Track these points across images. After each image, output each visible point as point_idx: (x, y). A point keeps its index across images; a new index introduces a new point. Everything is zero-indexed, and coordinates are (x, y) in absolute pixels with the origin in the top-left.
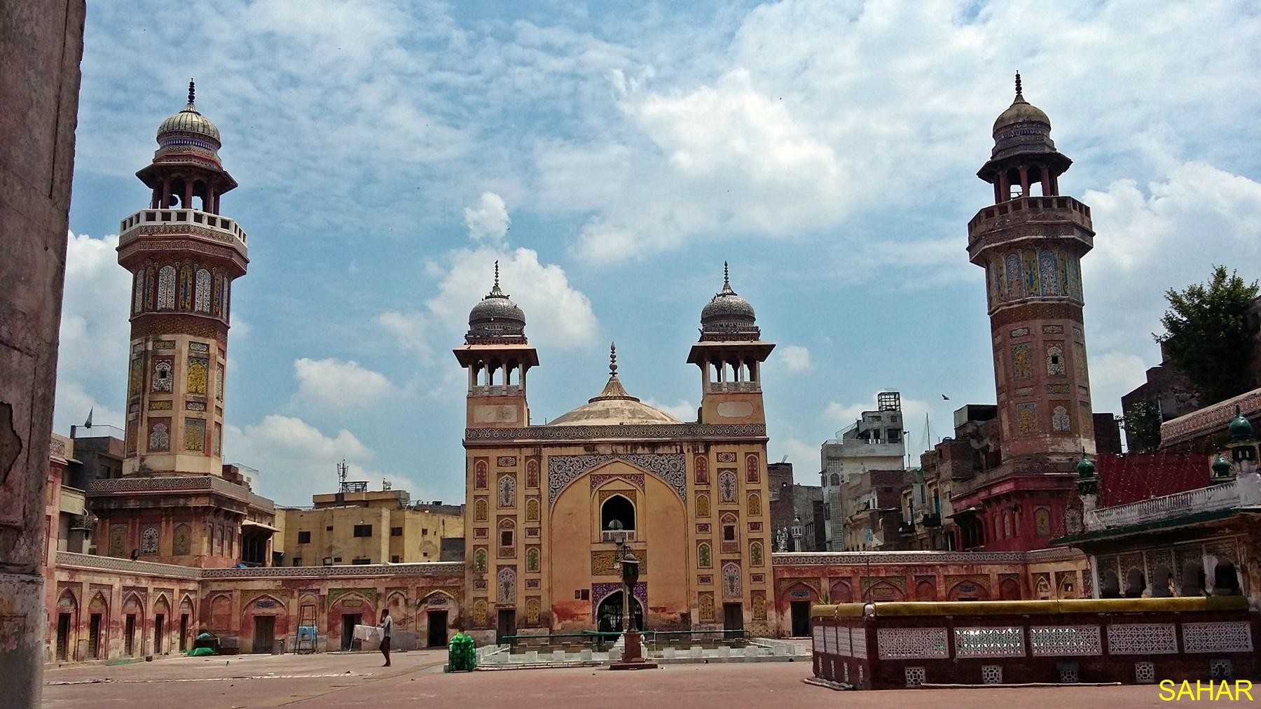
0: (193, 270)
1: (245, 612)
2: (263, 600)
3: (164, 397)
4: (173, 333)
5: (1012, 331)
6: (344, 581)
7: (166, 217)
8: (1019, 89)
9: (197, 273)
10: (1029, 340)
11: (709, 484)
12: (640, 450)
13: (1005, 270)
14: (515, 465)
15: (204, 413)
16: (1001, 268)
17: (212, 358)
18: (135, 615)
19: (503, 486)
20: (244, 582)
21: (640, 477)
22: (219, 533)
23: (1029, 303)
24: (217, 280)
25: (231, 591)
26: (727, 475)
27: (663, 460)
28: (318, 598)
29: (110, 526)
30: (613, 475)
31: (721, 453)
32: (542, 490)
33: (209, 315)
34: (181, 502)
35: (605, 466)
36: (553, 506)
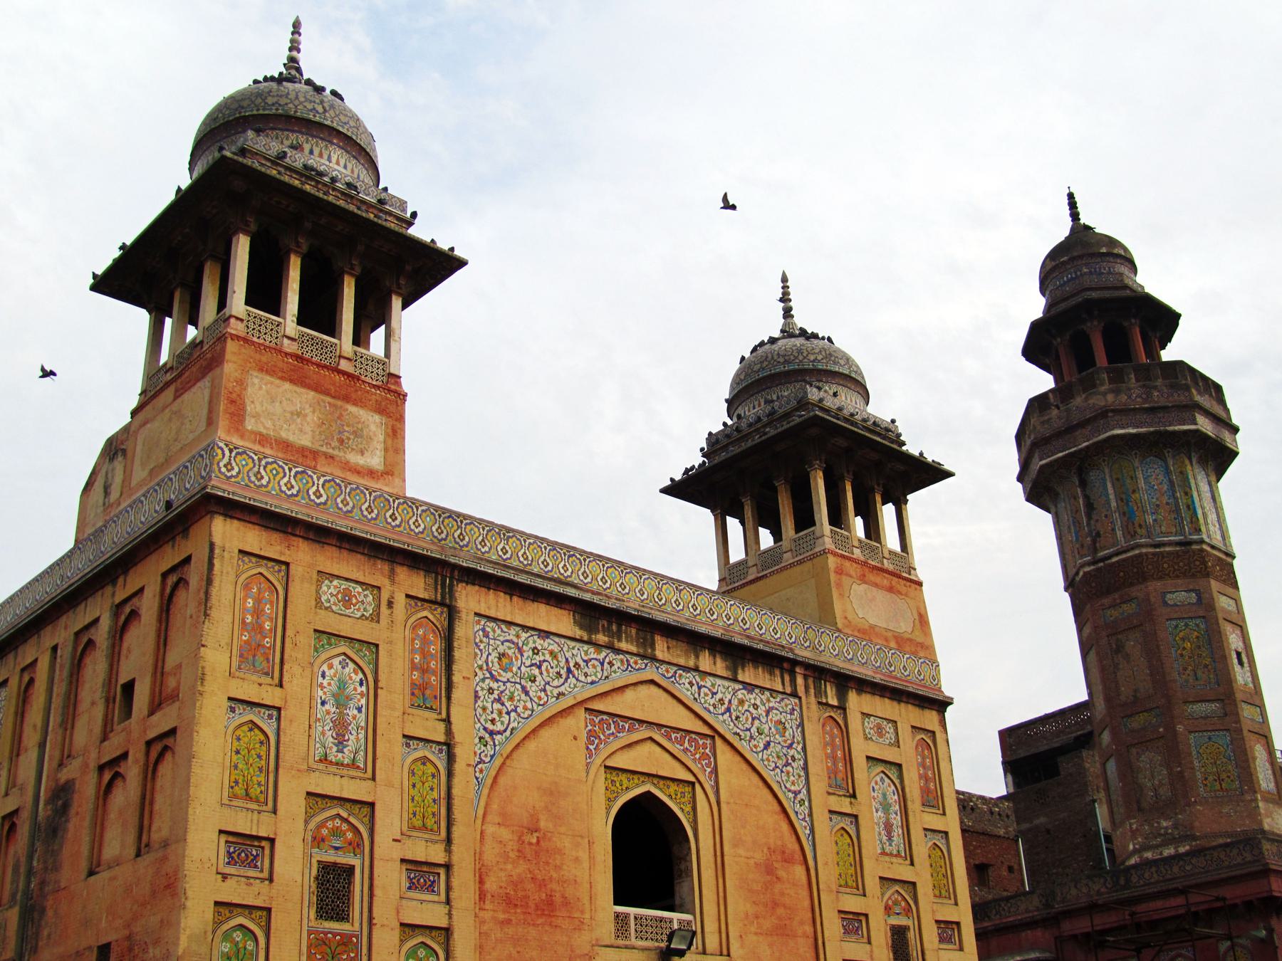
5: (1164, 594)
8: (1075, 216)
10: (1201, 613)
11: (854, 796)
12: (705, 662)
13: (1142, 483)
14: (376, 617)
16: (1075, 498)
19: (331, 685)
21: (705, 746)
23: (1195, 547)
26: (882, 779)
27: (756, 707)
30: (641, 722)
31: (868, 715)
32: (455, 728)
35: (621, 689)
36: (486, 791)
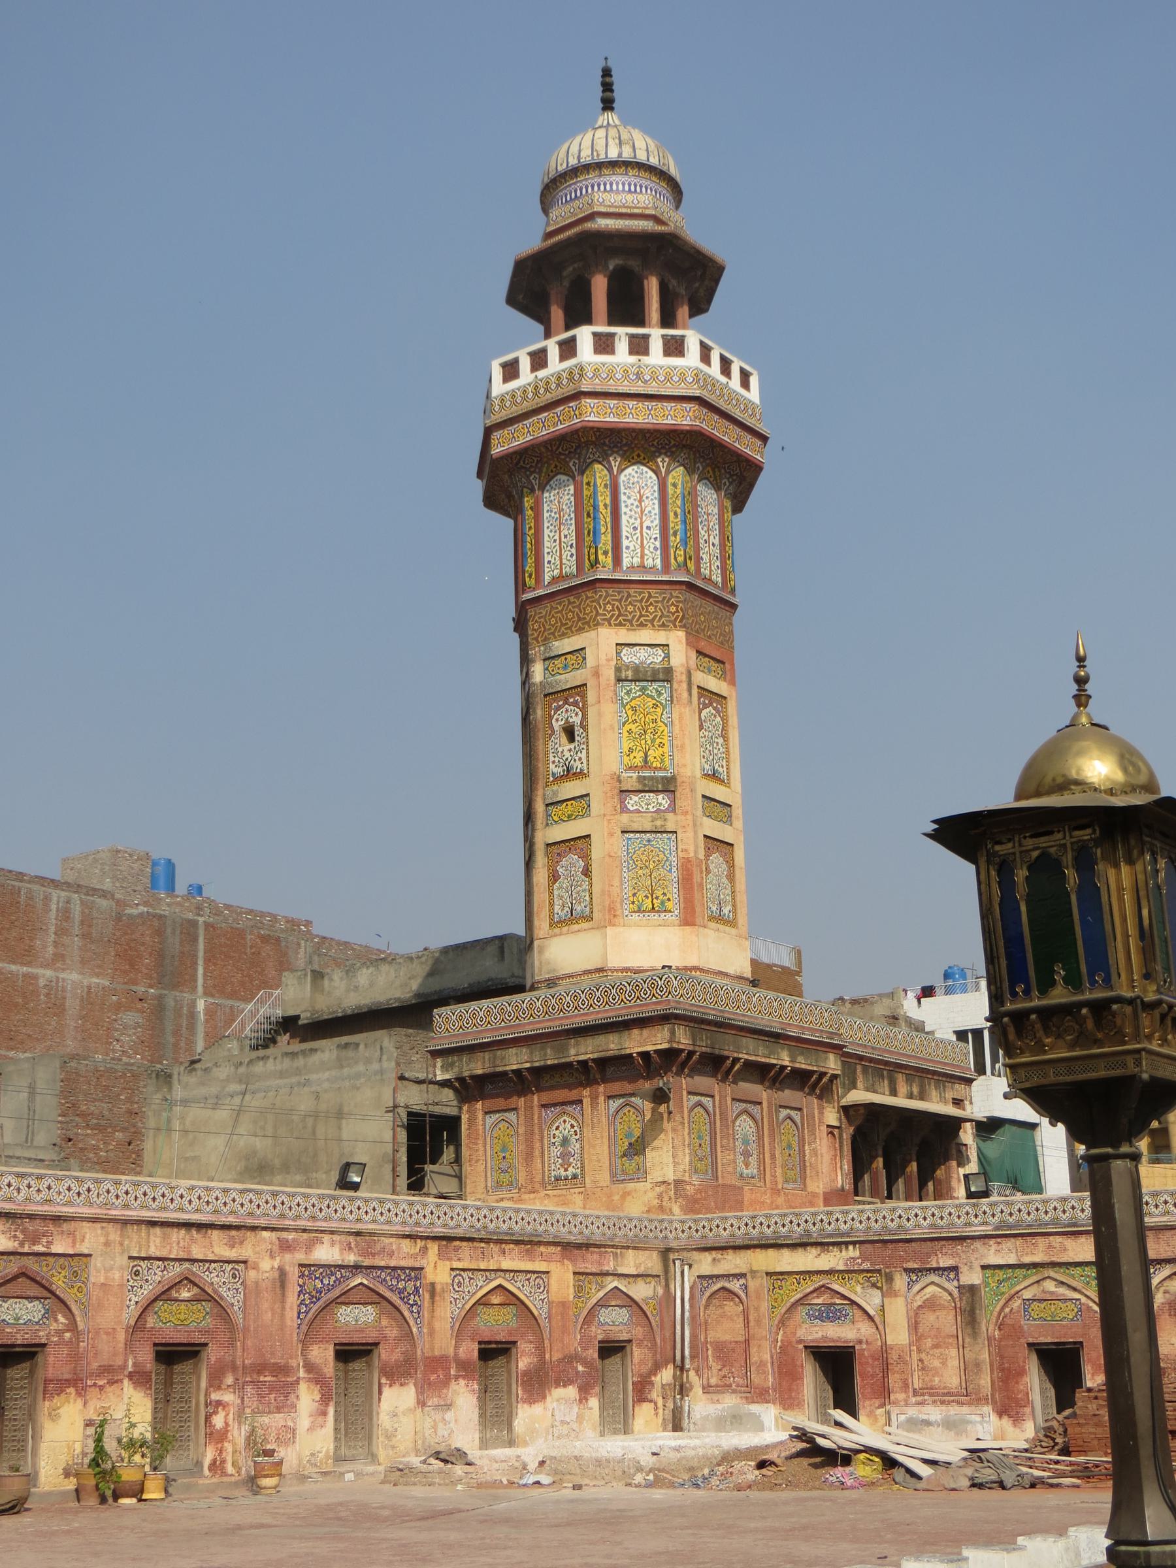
0: (610, 470)
1: (781, 1332)
2: (819, 1301)
3: (571, 789)
4: (580, 630)
6: (1019, 1241)
7: (539, 360)
9: (622, 478)
15: (670, 816)
17: (679, 676)
18: (376, 1344)
20: (771, 1252)
22: (745, 1126)
24: (675, 485)
25: (743, 1275)
28: (956, 1293)
29: (484, 1120)
33: (657, 572)
34: (612, 1044)
